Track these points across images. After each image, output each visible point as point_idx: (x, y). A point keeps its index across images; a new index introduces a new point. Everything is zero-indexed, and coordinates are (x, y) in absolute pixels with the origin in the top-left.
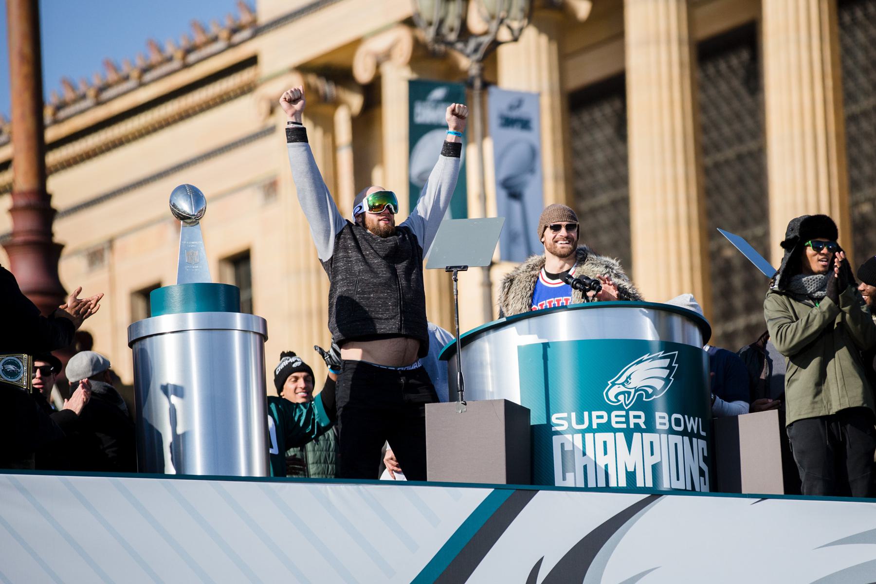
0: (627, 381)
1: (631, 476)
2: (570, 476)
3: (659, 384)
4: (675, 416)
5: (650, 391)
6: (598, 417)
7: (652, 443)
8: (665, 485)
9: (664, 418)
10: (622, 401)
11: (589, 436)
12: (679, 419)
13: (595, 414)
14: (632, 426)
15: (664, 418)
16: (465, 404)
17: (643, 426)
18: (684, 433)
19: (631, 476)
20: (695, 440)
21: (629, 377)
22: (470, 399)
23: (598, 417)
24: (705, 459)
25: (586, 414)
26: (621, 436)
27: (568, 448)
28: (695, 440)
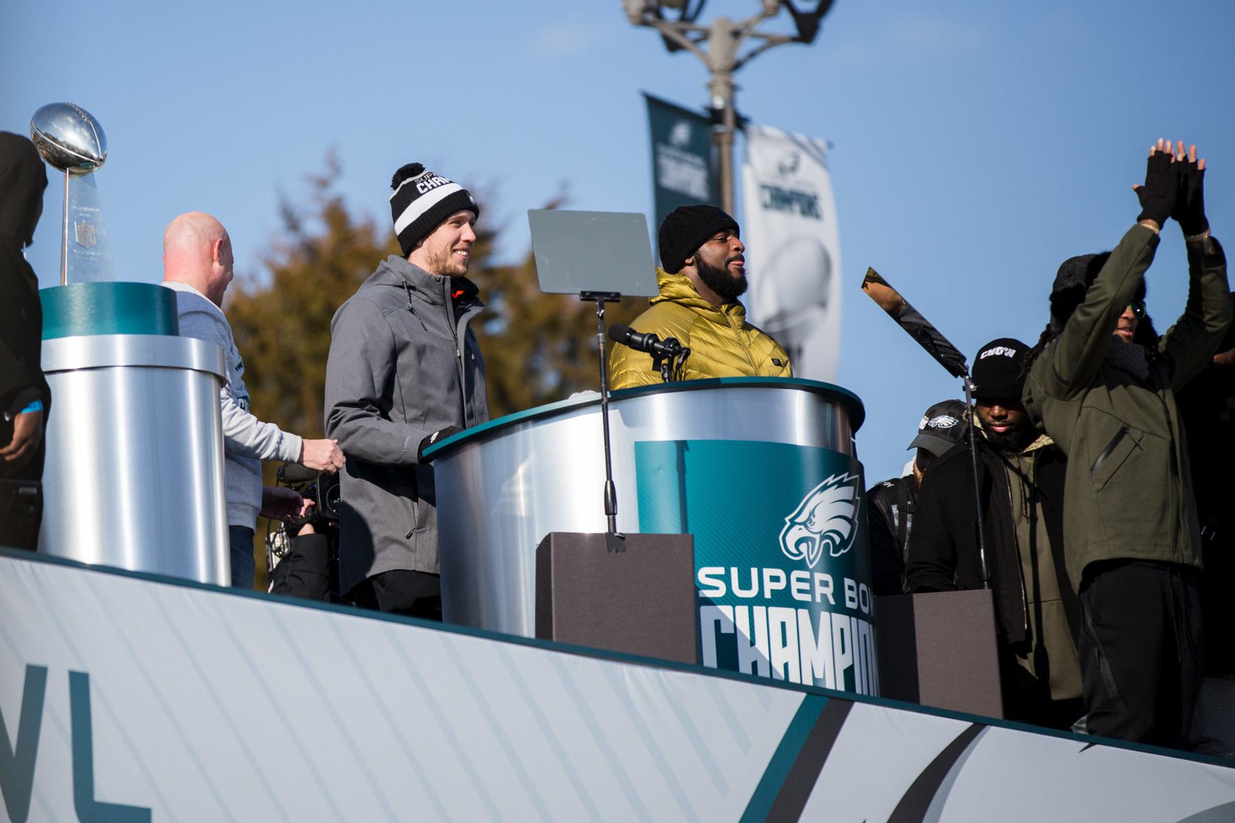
10: (805, 554)
11: (759, 611)
13: (768, 572)
23: (771, 579)
25: (754, 571)
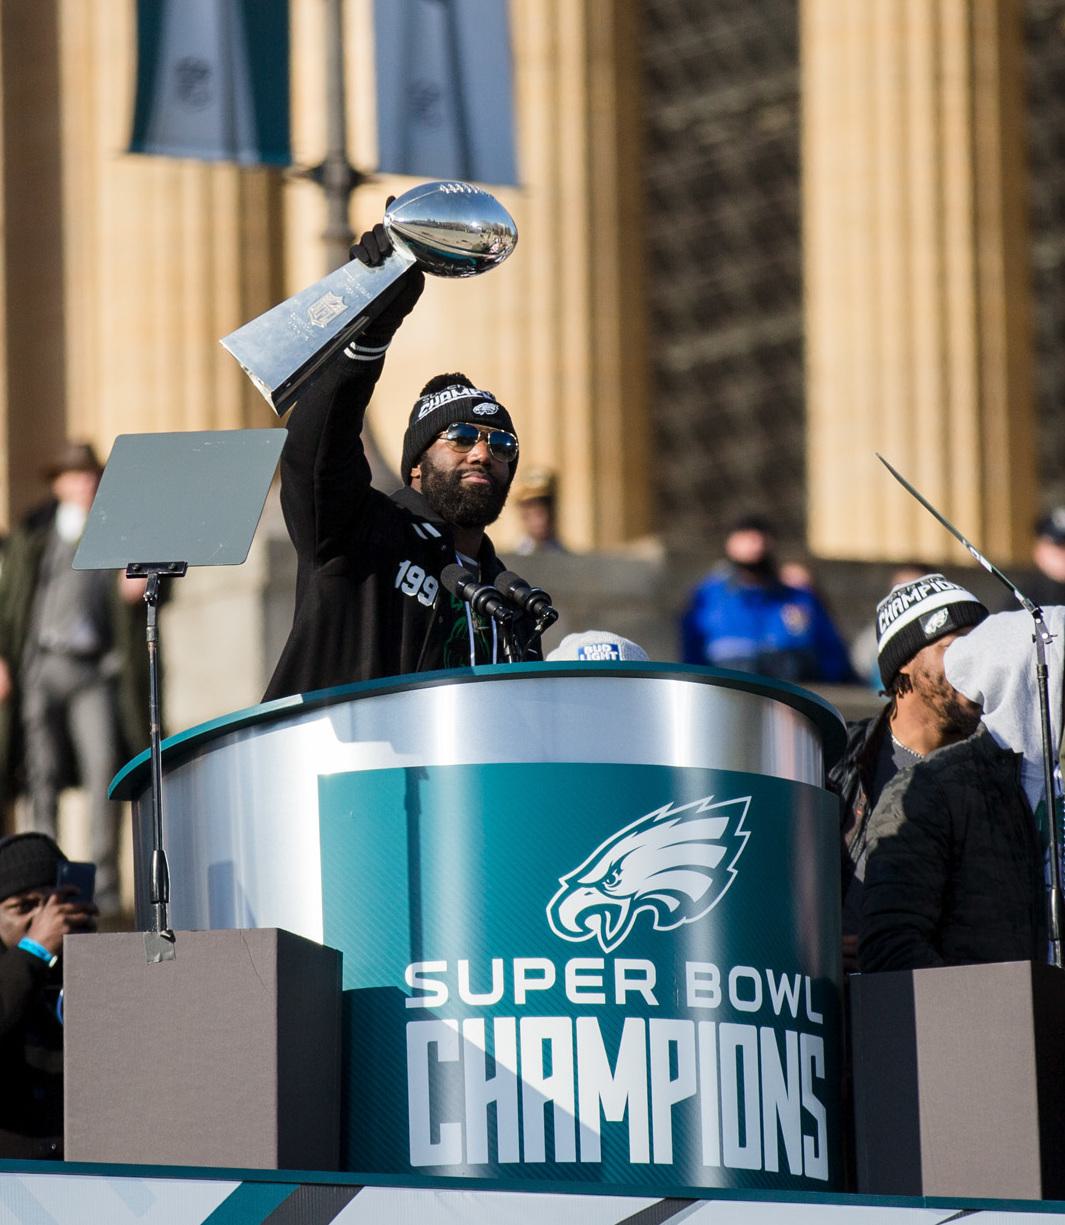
0: (609, 877)
1: (615, 1134)
2: (450, 1131)
3: (697, 886)
4: (739, 971)
5: (672, 904)
6: (531, 974)
7: (673, 1045)
8: (712, 1157)
9: (709, 977)
10: (597, 930)
11: (504, 1025)
12: (750, 981)
13: (521, 965)
14: (621, 999)
15: (709, 977)
16: (172, 939)
17: (652, 1000)
18: (763, 1017)
19: (615, 1134)
20: (791, 1036)
21: (616, 867)
22: (192, 926)
23: (531, 974)
24: (819, 1087)
25: (498, 965)
26: (589, 1026)
27: (447, 1054)
28: (791, 1036)
